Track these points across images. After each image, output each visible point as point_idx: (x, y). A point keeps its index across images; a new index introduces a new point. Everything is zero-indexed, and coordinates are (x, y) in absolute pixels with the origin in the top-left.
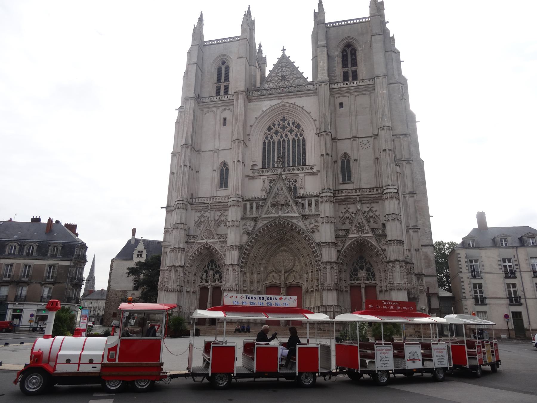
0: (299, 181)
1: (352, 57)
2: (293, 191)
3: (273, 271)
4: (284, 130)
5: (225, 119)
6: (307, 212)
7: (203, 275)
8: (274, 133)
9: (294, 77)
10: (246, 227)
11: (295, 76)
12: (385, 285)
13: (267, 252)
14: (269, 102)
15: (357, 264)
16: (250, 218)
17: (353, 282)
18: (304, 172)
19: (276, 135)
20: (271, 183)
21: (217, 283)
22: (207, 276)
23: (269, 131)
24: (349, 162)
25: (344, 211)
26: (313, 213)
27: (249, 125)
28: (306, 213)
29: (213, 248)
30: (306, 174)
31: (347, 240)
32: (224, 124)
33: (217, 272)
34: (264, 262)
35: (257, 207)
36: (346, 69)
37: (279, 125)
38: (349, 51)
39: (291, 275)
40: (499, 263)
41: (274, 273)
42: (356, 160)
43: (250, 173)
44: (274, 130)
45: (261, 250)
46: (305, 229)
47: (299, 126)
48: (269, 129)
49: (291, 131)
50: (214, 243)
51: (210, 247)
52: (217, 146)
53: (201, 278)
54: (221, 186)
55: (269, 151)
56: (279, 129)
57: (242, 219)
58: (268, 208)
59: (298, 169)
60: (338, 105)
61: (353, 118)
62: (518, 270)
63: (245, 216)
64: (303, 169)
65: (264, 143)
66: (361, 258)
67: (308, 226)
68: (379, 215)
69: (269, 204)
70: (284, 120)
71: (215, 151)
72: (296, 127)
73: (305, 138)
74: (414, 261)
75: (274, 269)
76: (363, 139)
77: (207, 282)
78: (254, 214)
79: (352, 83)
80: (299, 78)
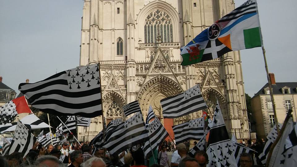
2: (167, 59)
5: (118, 9)
7: (108, 111)
10: (138, 81)
12: (225, 116)
13: (151, 96)
19: (153, 21)
20: (152, 52)
21: (118, 116)
23: (148, 19)
27: (136, 14)
29: (117, 95)
31: (203, 89)
32: (118, 13)
33: (118, 109)
34: (148, 102)
35: (146, 69)
37: (155, 15)
40: (284, 103)
43: (138, 46)
44: (151, 18)
46: (177, 83)
47: (168, 16)
48: (149, 17)
50: (118, 91)
51: (114, 94)
52: (113, 27)
53: (107, 113)
54: (118, 54)
55: (149, 32)
57: (136, 75)
59: (169, 45)
60: (193, 5)
61: (202, 13)
62: (293, 107)
63: (138, 74)
64: (172, 45)
65: (145, 26)
69: (153, 66)
70: (158, 12)
71: (114, 30)
74: (241, 102)
75: (155, 107)
77: (111, 116)
78: (144, 73)
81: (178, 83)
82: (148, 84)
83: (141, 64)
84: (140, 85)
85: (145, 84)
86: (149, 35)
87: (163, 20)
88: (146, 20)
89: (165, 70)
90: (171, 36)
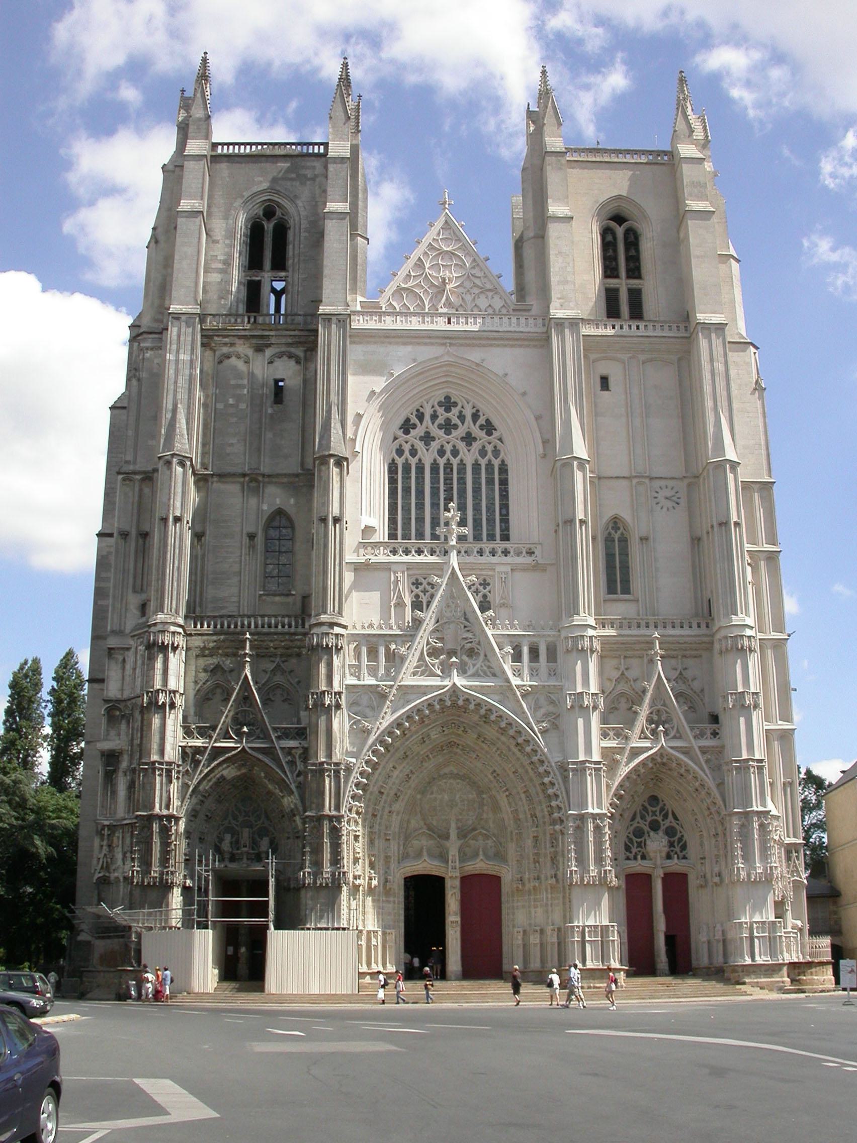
0: (496, 585)
1: (627, 250)
4: (448, 433)
8: (421, 439)
9: (475, 285)
11: (478, 282)
14: (409, 348)
15: (643, 817)
17: (632, 863)
18: (508, 559)
22: (236, 844)
23: (407, 432)
24: (624, 541)
25: (616, 674)
33: (263, 832)
34: (396, 807)
36: (613, 283)
37: (434, 417)
38: (620, 231)
42: (644, 539)
44: (419, 431)
45: (396, 773)
47: (489, 428)
48: (407, 427)
49: (469, 439)
55: (407, 490)
56: (435, 431)
64: (506, 553)
66: (654, 800)
68: (702, 690)
70: (448, 404)
72: (481, 427)
73: (508, 462)
76: (663, 483)
79: (634, 327)
80: (490, 290)
87: (469, 439)
88: (395, 439)
89: (474, 665)
90: (504, 512)
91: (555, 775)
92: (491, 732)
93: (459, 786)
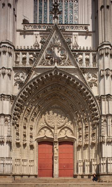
3: (45, 127)
6: (84, 65)
10: (18, 78)
16: (23, 68)
26: (92, 67)
28: (85, 67)
30: (81, 34)
39: (63, 131)
41: (45, 129)
46: (84, 82)
55: (41, 11)
57: (15, 69)
58: (43, 59)
67: (86, 79)
75: (46, 125)
78: (28, 65)
81: (86, 82)
82: (34, 83)
83: (24, 51)
84: (21, 84)
85: (28, 84)
86: (40, 15)
91: (96, 101)
92: (70, 88)
93: (59, 111)
